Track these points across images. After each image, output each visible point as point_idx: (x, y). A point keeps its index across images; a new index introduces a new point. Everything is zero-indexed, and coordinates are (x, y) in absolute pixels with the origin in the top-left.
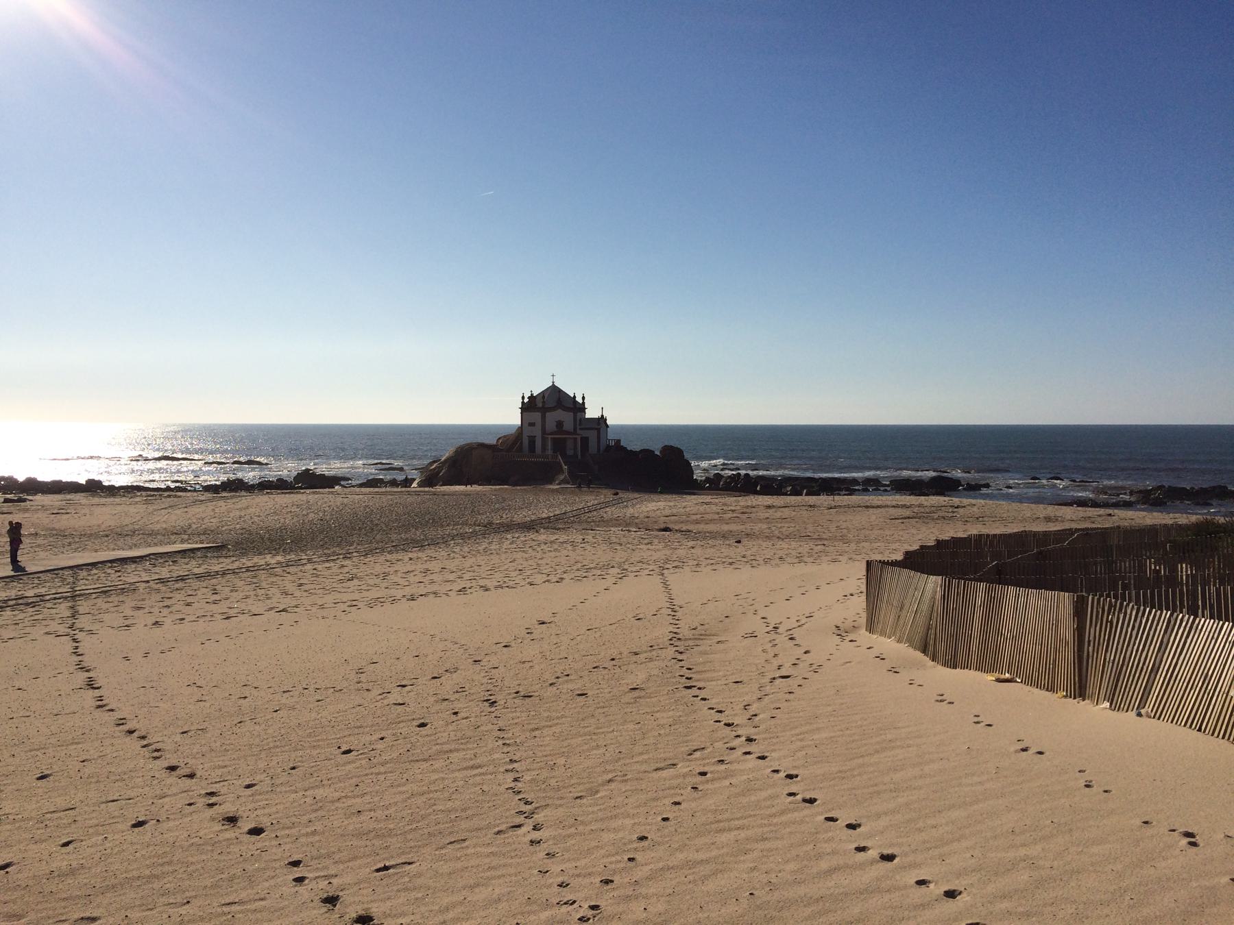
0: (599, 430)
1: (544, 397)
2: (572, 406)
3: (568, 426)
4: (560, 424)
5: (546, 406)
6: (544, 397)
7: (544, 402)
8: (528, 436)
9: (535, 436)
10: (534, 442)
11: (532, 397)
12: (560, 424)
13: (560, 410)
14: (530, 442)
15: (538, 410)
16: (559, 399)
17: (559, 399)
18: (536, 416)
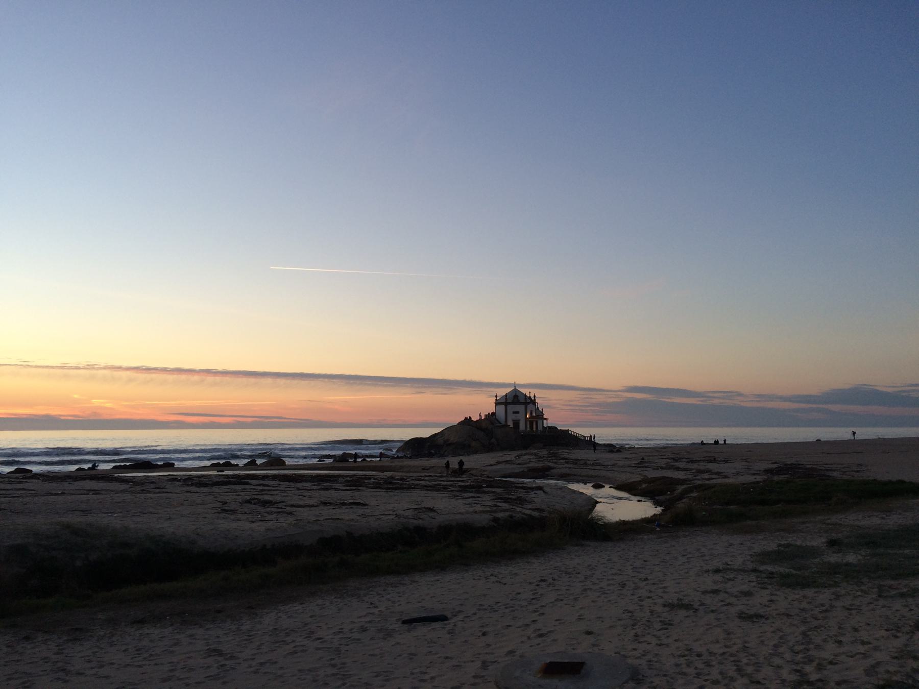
8: (513, 420)
9: (519, 420)
10: (519, 423)
14: (514, 424)
17: (530, 397)
18: (521, 408)
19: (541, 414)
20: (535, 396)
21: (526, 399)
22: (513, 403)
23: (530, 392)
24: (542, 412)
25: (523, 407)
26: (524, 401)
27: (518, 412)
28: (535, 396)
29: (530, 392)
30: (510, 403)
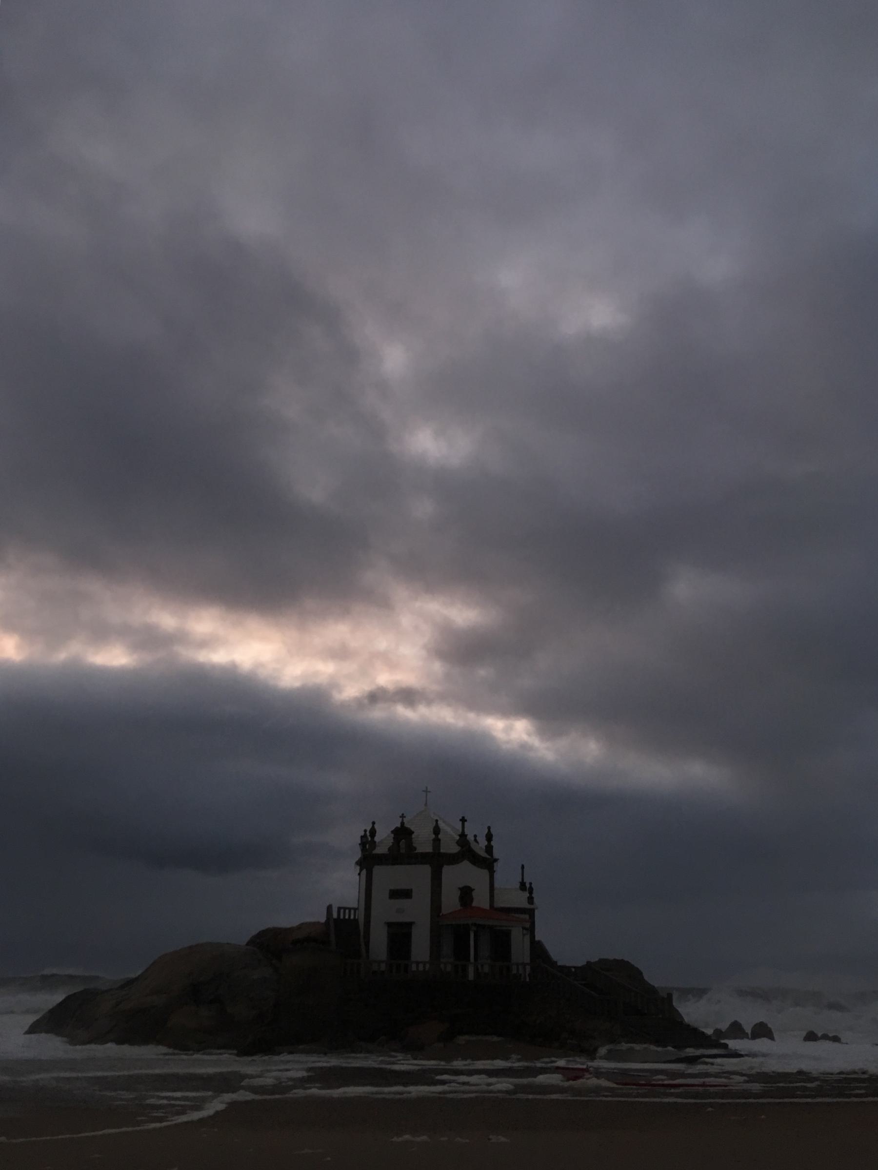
0: (531, 913)
1: (437, 830)
2: (483, 854)
3: (481, 900)
4: (466, 894)
5: (442, 851)
6: (437, 830)
7: (437, 841)
8: (390, 925)
9: (410, 925)
10: (408, 936)
11: (402, 833)
12: (466, 894)
13: (466, 866)
15: (423, 858)
16: (463, 835)
17: (463, 835)
19: (525, 905)
20: (489, 837)
21: (437, 841)
22: (394, 857)
23: (463, 820)
24: (531, 900)
25: (426, 870)
26: (429, 849)
27: (406, 894)
28: (489, 837)
29: (463, 820)
30: (382, 860)
